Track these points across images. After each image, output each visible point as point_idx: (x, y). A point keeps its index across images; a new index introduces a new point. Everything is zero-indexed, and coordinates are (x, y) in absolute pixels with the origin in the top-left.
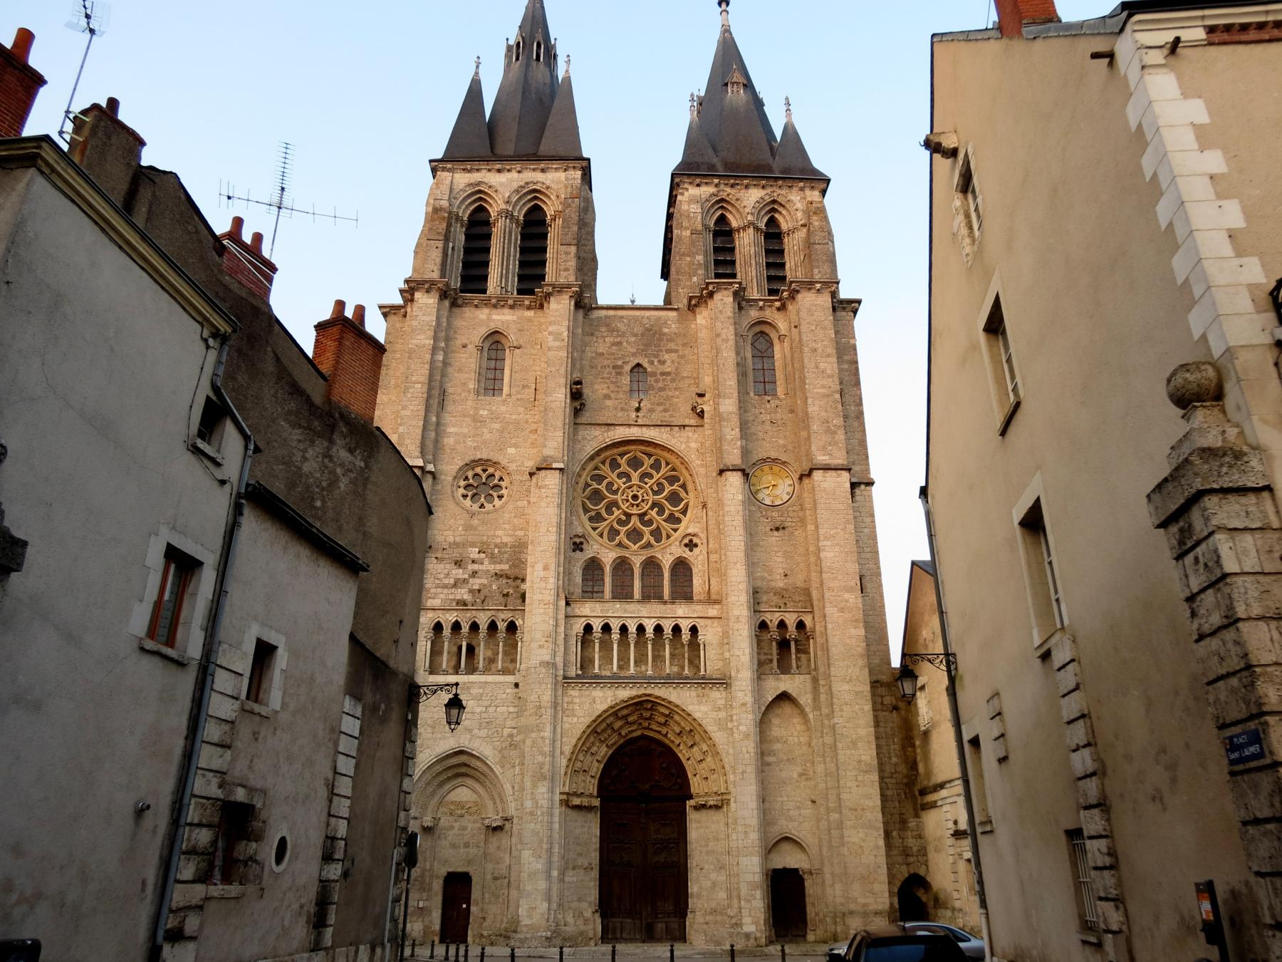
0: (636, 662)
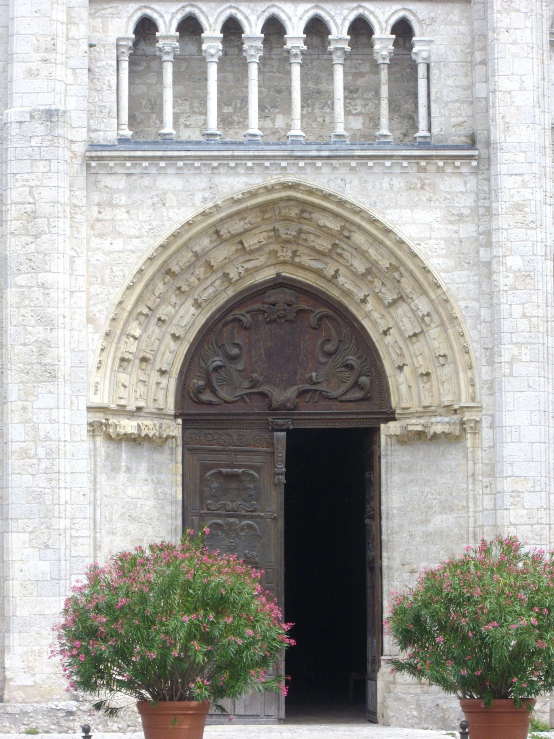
0: (262, 107)
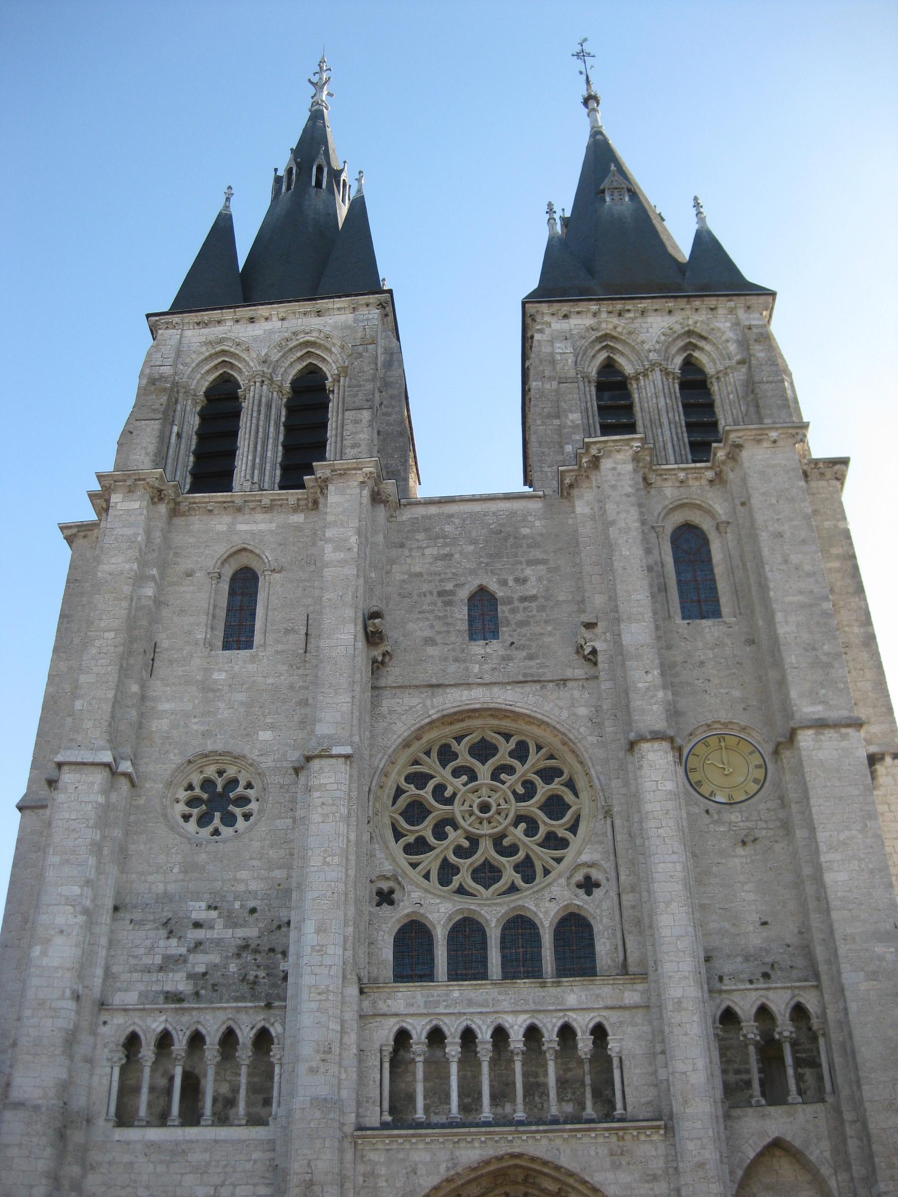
0: (494, 1097)
